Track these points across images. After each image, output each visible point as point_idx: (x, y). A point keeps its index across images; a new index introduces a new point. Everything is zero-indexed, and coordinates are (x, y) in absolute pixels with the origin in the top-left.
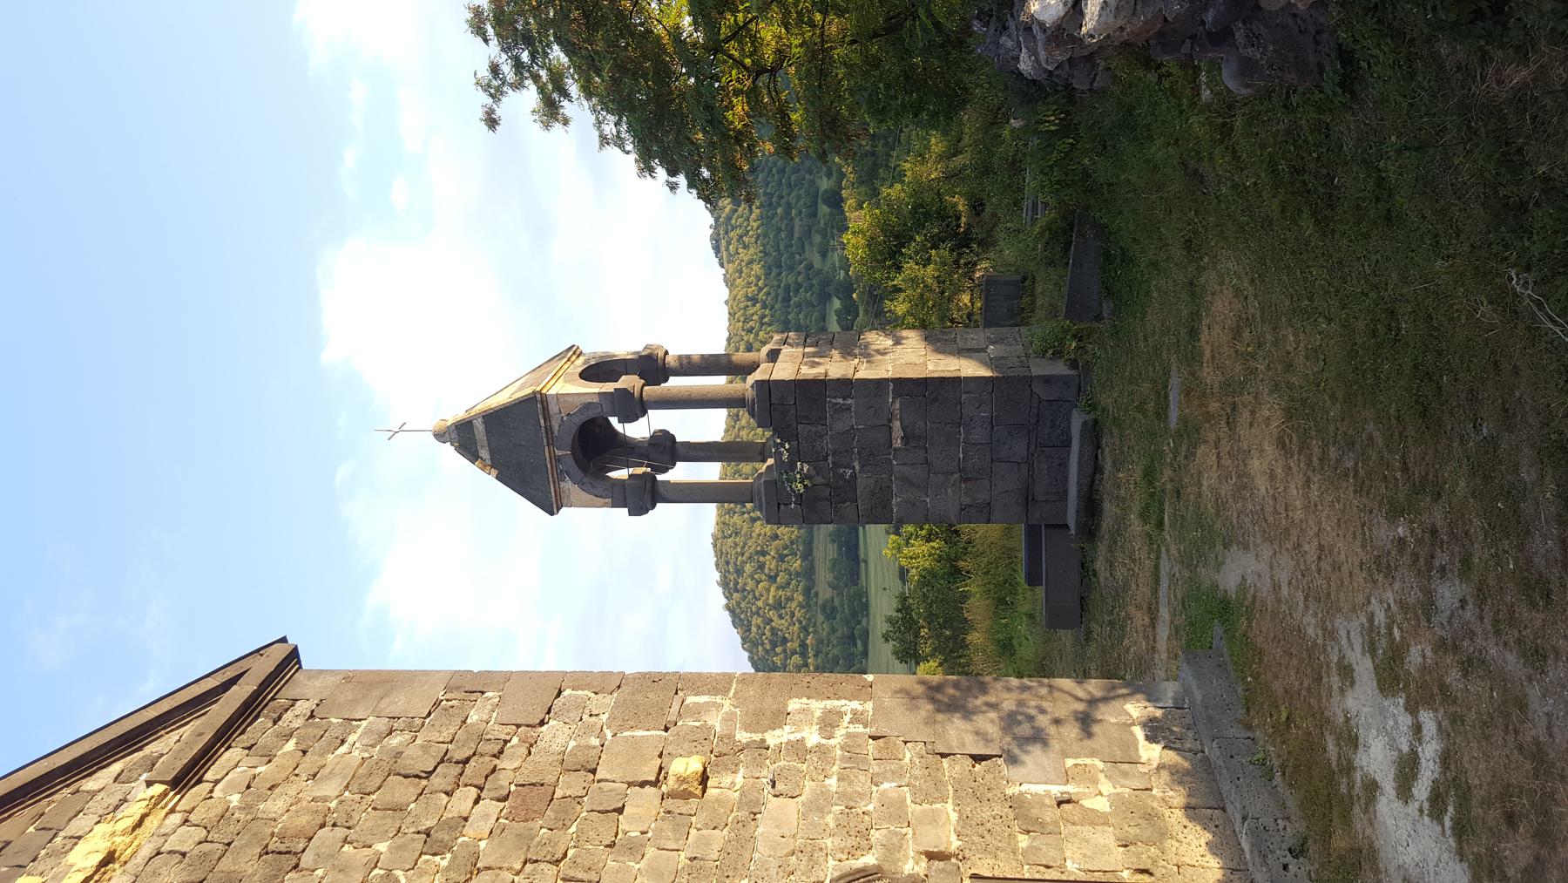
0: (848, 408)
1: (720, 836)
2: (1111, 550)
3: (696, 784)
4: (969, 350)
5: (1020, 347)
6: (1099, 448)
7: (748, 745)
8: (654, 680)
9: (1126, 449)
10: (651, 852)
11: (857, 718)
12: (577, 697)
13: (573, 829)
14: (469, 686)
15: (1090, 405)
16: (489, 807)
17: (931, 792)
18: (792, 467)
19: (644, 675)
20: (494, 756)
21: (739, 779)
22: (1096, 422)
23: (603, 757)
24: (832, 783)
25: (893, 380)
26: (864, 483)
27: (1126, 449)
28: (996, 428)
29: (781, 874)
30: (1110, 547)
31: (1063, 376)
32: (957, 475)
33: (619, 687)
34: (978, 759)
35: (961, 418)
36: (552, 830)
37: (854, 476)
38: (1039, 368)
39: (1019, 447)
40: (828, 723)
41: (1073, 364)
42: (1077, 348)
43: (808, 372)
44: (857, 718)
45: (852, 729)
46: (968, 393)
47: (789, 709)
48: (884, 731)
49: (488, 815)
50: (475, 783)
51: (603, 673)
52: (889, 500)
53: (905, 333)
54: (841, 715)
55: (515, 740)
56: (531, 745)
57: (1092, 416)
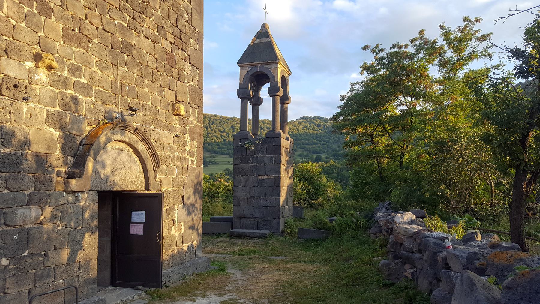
0: (271, 162)
1: (164, 119)
2: (227, 242)
3: (177, 112)
4: (287, 200)
5: (287, 215)
6: (258, 238)
7: (186, 128)
8: (201, 100)
9: (259, 246)
10: (160, 98)
11: (193, 162)
12: (197, 74)
13: (165, 74)
14: (199, 40)
15: (271, 236)
16: (169, 47)
17: (175, 183)
18: (253, 144)
19: (202, 96)
20: (182, 48)
21: (177, 126)
22: (266, 237)
23: (182, 83)
24: (177, 154)
25: (280, 176)
26: (247, 167)
27: (259, 246)
28: (264, 208)
29: (156, 138)
30: (228, 242)
31: (280, 228)
32: (249, 195)
33: (199, 88)
34: (183, 197)
35: (267, 197)
36: (164, 67)
37: (249, 163)
38: (282, 221)
39: (258, 214)
40: (191, 153)
41: (283, 231)
42: (288, 232)
43: (283, 149)
44: (193, 162)
45: (190, 160)
46: (275, 200)
47: (194, 142)
48: (189, 170)
49: (168, 46)
50: (176, 42)
51: (203, 83)
52: (241, 174)
53: (292, 180)
54: (193, 157)
55: (186, 55)
56: (184, 60)
57: (268, 236)
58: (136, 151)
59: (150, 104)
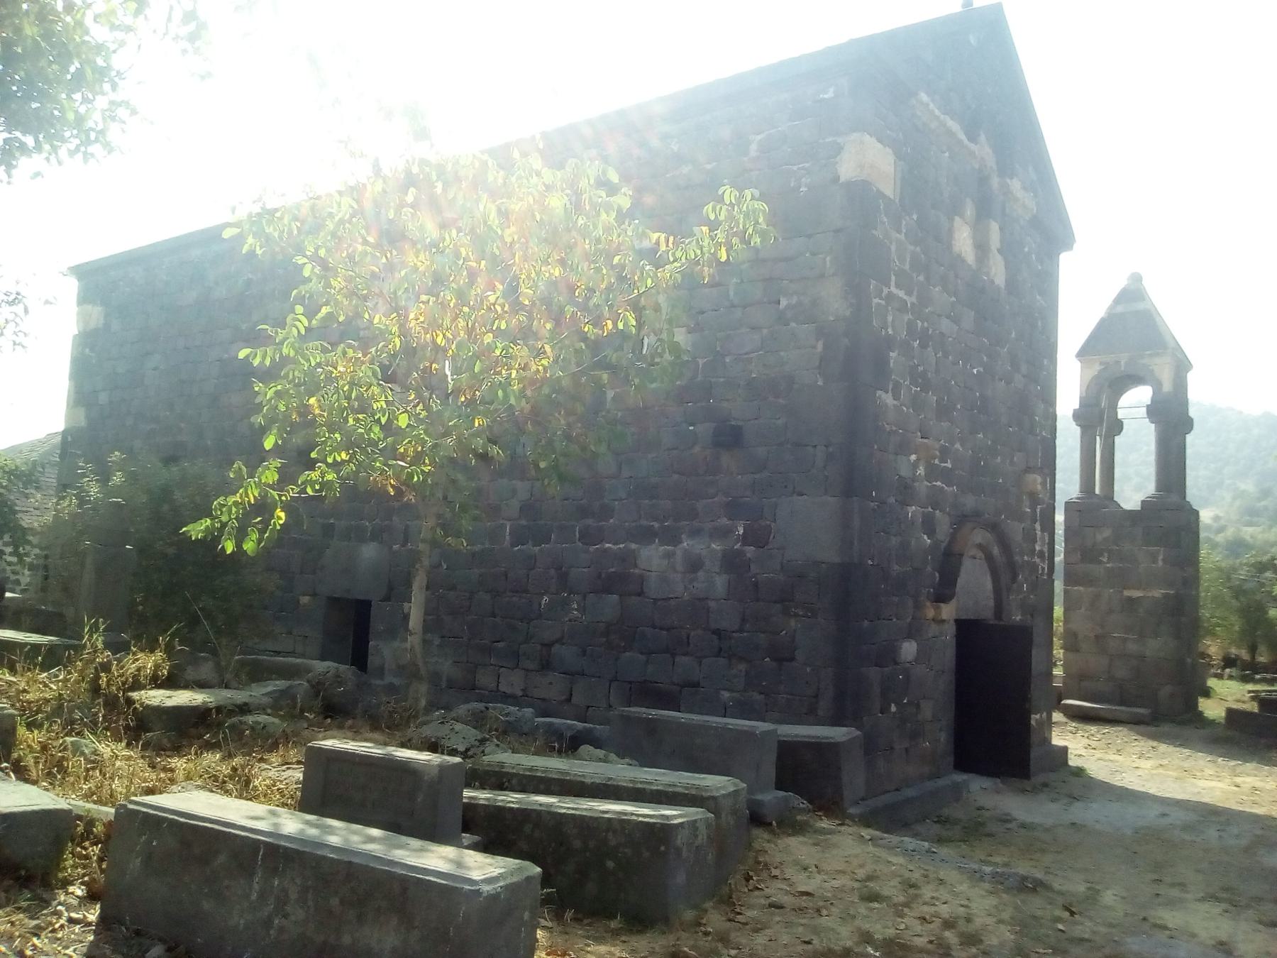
0: (1155, 561)
37: (1100, 562)
39: (1121, 672)
44: (1043, 569)
54: (1044, 562)
58: (989, 558)
59: (1001, 481)
